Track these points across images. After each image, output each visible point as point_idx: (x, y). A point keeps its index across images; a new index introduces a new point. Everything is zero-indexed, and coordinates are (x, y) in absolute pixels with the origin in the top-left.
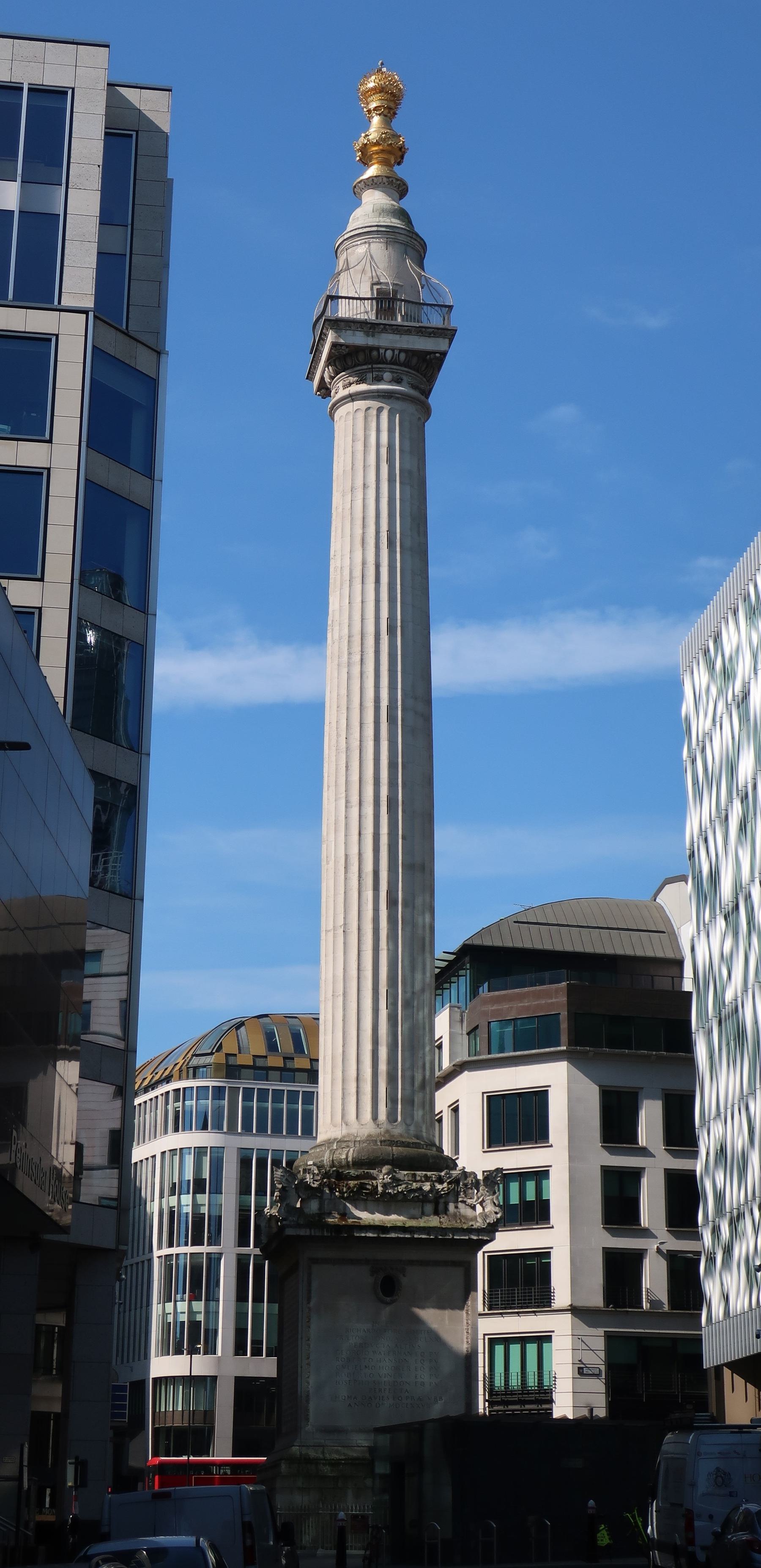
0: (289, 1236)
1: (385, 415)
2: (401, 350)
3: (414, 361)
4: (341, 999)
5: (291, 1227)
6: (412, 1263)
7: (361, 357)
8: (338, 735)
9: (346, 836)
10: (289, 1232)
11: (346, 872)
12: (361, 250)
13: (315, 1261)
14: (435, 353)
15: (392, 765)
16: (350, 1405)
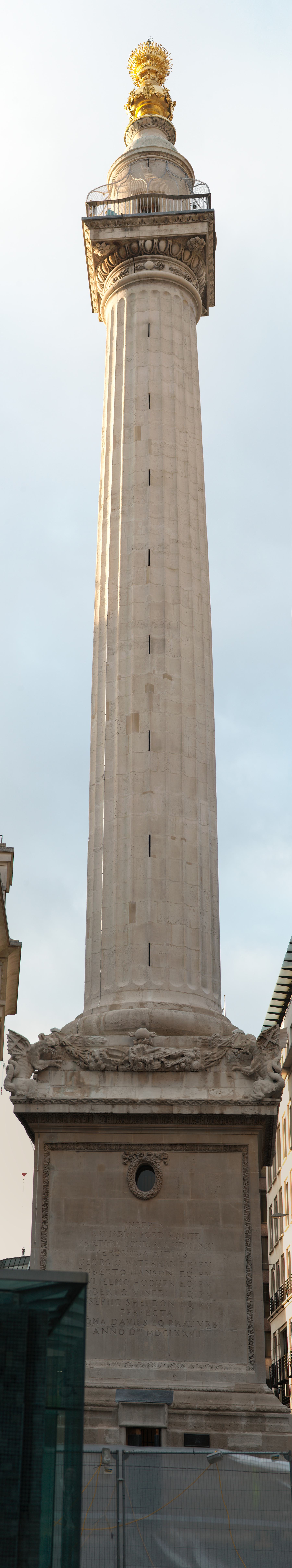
6: (173, 1147)
13: (53, 1146)
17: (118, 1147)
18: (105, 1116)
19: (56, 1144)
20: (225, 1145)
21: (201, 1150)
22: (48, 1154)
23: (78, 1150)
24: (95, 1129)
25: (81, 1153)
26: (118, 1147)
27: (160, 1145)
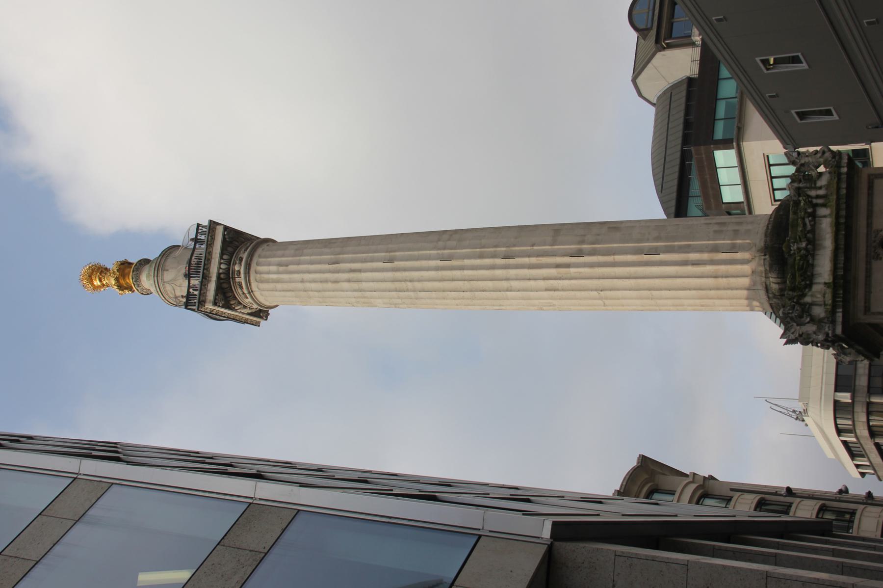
0: (843, 331)
1: (260, 268)
2: (221, 258)
3: (230, 249)
4: (654, 292)
5: (834, 330)
6: (869, 225)
7: (225, 286)
8: (463, 298)
9: (532, 291)
10: (839, 330)
11: (557, 290)
12: (169, 288)
14: (224, 235)
15: (481, 256)
17: (868, 263)
19: (865, 307)
26: (868, 263)
27: (867, 234)
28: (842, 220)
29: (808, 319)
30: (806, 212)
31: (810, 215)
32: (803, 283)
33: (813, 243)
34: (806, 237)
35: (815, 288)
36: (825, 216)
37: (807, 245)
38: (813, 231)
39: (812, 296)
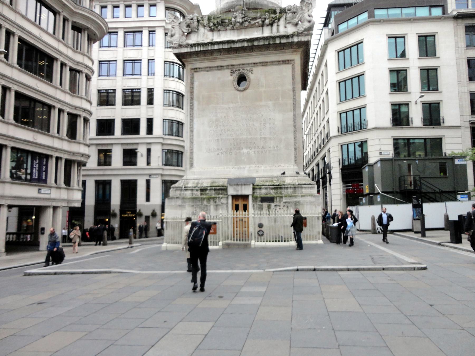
16: (218, 154)
18: (220, 51)
20: (283, 61)
21: (270, 65)
22: (193, 74)
23: (208, 71)
24: (215, 59)
25: (209, 73)
28: (256, 43)
29: (184, 31)
30: (265, 19)
31: (263, 22)
32: (212, 24)
33: (242, 26)
34: (245, 21)
35: (210, 34)
36: (263, 33)
37: (239, 22)
38: (253, 26)
39: (204, 33)
